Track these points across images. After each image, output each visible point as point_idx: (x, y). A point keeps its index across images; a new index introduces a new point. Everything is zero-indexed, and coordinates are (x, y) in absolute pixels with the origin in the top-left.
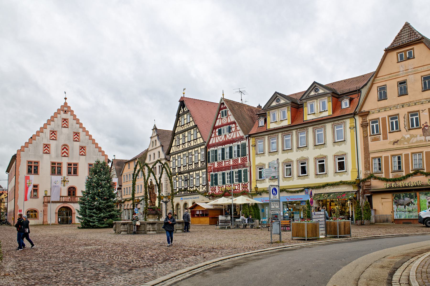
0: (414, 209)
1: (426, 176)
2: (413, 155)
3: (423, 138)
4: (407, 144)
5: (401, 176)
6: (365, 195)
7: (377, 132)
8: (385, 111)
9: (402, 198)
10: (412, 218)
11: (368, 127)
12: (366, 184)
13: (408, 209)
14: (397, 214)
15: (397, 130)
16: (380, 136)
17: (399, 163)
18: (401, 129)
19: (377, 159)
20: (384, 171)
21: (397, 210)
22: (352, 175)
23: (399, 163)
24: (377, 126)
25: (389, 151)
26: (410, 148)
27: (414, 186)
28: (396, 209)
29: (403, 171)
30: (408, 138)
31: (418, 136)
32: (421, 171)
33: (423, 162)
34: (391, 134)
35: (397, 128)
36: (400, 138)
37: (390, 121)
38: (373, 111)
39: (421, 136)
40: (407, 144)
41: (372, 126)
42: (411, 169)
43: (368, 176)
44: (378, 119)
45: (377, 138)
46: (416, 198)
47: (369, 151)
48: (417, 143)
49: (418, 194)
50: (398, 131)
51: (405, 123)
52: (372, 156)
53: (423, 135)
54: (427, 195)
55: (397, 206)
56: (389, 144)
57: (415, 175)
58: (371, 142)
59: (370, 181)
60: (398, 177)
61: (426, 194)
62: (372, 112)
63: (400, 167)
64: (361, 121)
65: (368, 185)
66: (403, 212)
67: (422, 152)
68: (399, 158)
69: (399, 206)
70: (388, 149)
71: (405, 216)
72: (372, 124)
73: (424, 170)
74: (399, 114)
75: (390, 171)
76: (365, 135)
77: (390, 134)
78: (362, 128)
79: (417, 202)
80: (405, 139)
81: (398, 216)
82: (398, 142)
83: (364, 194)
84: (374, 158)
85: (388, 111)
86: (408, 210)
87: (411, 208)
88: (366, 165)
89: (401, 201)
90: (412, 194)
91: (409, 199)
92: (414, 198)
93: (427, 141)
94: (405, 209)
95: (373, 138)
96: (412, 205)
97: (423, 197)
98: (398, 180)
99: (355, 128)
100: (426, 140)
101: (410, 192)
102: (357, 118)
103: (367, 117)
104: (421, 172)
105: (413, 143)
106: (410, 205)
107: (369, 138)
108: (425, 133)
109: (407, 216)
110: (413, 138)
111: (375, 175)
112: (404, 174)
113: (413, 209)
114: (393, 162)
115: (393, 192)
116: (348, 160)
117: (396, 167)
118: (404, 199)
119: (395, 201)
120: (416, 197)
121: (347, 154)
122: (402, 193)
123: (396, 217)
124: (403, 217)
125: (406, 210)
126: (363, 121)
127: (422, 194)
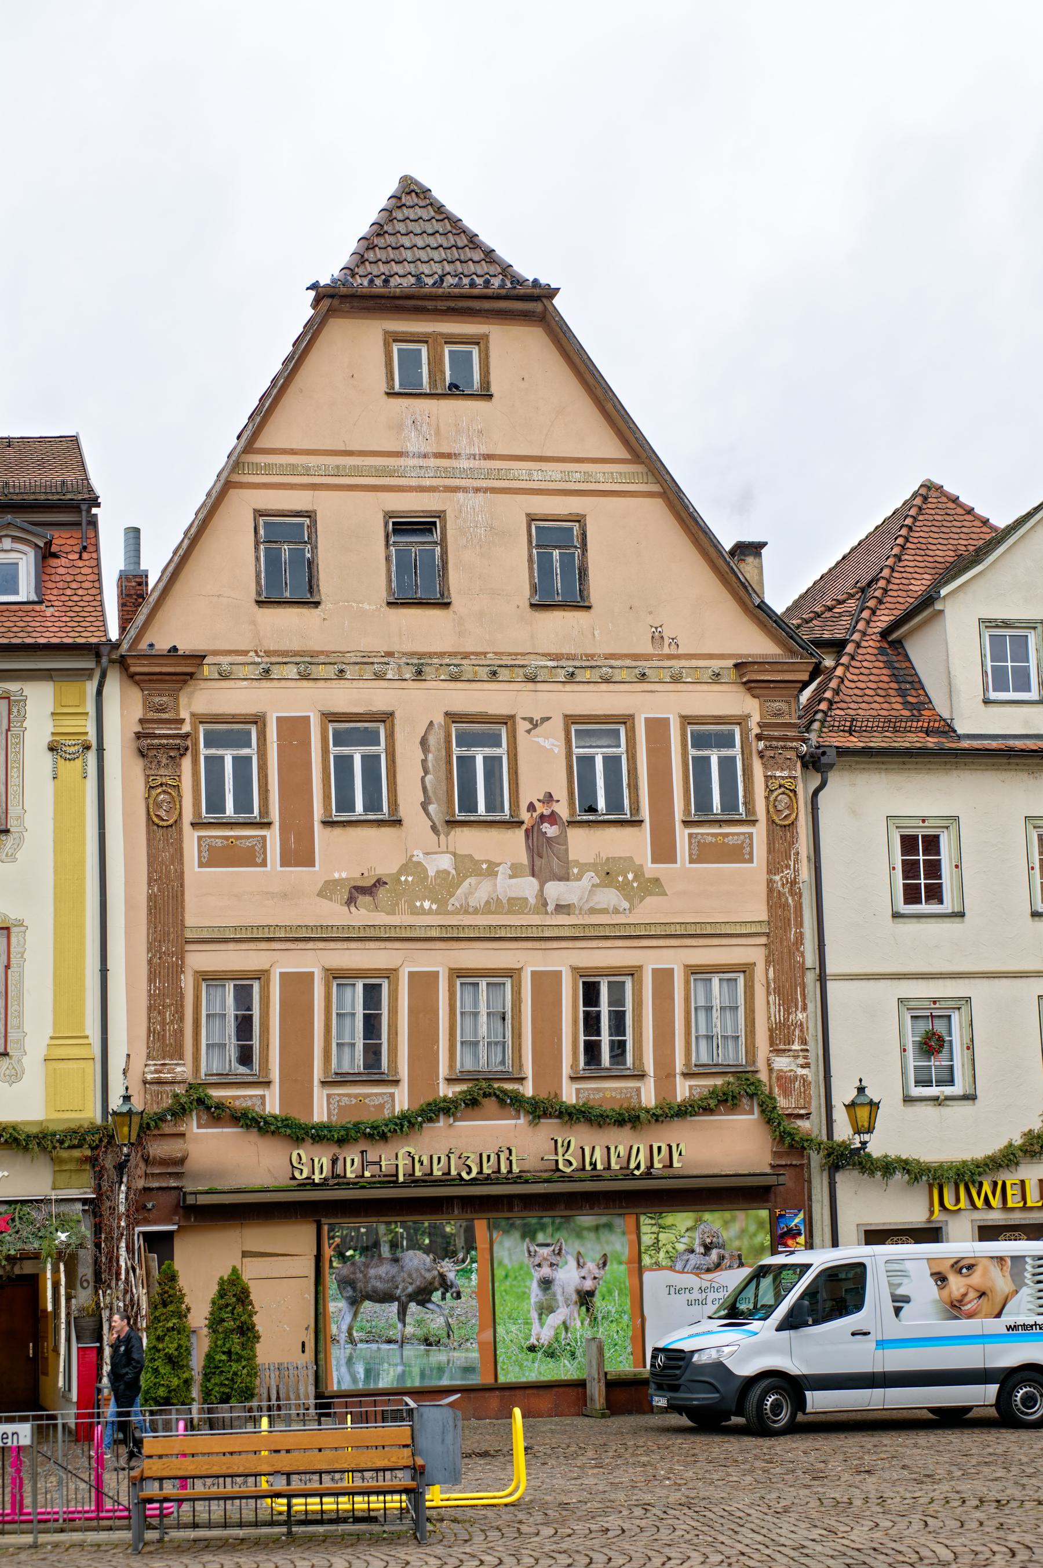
0: (454, 1327)
1: (530, 1123)
2: (458, 982)
3: (527, 887)
4: (430, 912)
5: (387, 1113)
6: (138, 1229)
7: (243, 802)
8: (305, 677)
9: (385, 1251)
10: (445, 1382)
11: (186, 763)
12: (158, 1149)
13: (419, 1323)
14: (350, 1361)
15: (371, 817)
16: (264, 838)
17: (371, 1025)
18: (403, 812)
19: (230, 987)
20: (275, 1075)
21: (350, 1334)
22: (53, 1086)
23: (371, 1025)
24: (242, 764)
25: (321, 945)
26: (453, 938)
27: (474, 1182)
28: (344, 1327)
29: (396, 1082)
30: (442, 874)
31: (500, 869)
32: (508, 1086)
33: (517, 1035)
34: (338, 831)
35: (372, 803)
36: (394, 870)
37: (334, 750)
38: (224, 660)
39: (516, 872)
40: (430, 912)
41: (207, 758)
42: (443, 1071)
43: (176, 1096)
44: (258, 720)
45: (248, 843)
46: (468, 1252)
47: (183, 927)
48: (490, 912)
49: (481, 1227)
50: (380, 823)
51: (429, 778)
52: (200, 959)
53: (528, 870)
54: (533, 1238)
55: (354, 1302)
56: (320, 894)
57: (469, 1110)
58: (201, 865)
59: (182, 1135)
60: (368, 1117)
61: (529, 1233)
62: (214, 669)
63: (372, 1053)
64: (138, 712)
65: (164, 1162)
66: (389, 1341)
67: (513, 974)
68: (372, 994)
69: (367, 1304)
70: (312, 927)
71: (400, 1369)
72: (212, 751)
73: (521, 1080)
74: (391, 714)
75: (318, 1074)
76: (162, 813)
77: (329, 829)
78: (138, 766)
79: (474, 1283)
80: (427, 877)
81: (360, 1369)
82: (382, 893)
83: (138, 1223)
84: (212, 979)
85: (321, 684)
86: (420, 1333)
87: (441, 1321)
88: (163, 1024)
89: (380, 1273)
90: (448, 1229)
91: (428, 1259)
92: (461, 1256)
93: (550, 908)
94: (400, 1326)
95: (219, 843)
96: (444, 1298)
97: (509, 1250)
98: (371, 1136)
99: (92, 757)
100: (545, 904)
101: (437, 1220)
102: (113, 687)
103: (183, 700)
104: (505, 1092)
105: (467, 912)
106: (436, 1296)
107: (191, 838)
108: (541, 856)
109: (416, 1371)
110: (472, 880)
111: (216, 1093)
112: (401, 1100)
113: (448, 1325)
114: (334, 1016)
115: (335, 1215)
116: (21, 975)
117: (347, 1050)
118: (396, 1260)
119: (345, 1270)
120: (470, 1245)
121: (13, 930)
122: (388, 1223)
123: (340, 1379)
124: (385, 1381)
125: (409, 1330)
126: (151, 715)
127: (506, 1232)
